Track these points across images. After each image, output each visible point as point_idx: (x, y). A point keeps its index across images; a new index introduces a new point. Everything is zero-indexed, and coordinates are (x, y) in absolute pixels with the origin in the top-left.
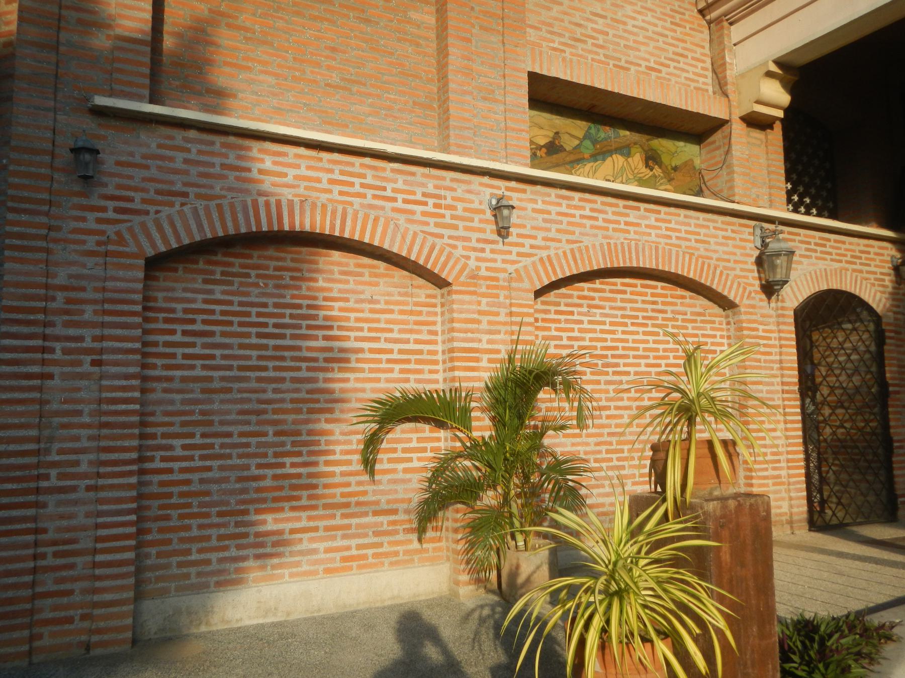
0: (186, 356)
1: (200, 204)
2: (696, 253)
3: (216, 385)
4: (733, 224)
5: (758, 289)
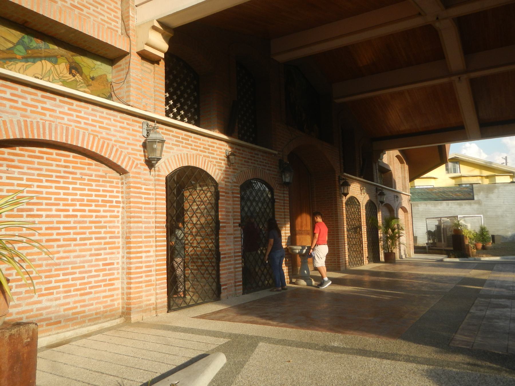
2: (99, 135)
4: (129, 120)
5: (144, 163)
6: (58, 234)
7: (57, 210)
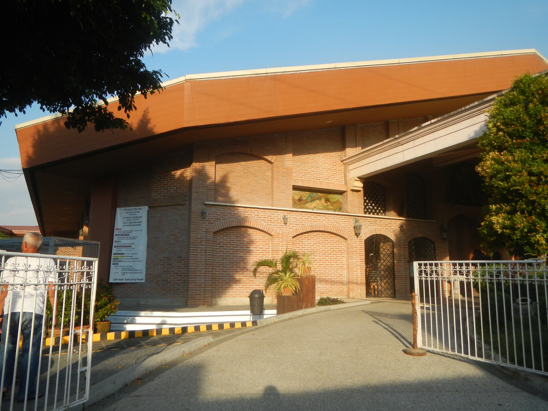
0: (219, 251)
1: (223, 221)
2: (336, 226)
3: (225, 257)
4: (347, 218)
6: (323, 262)
7: (322, 254)
